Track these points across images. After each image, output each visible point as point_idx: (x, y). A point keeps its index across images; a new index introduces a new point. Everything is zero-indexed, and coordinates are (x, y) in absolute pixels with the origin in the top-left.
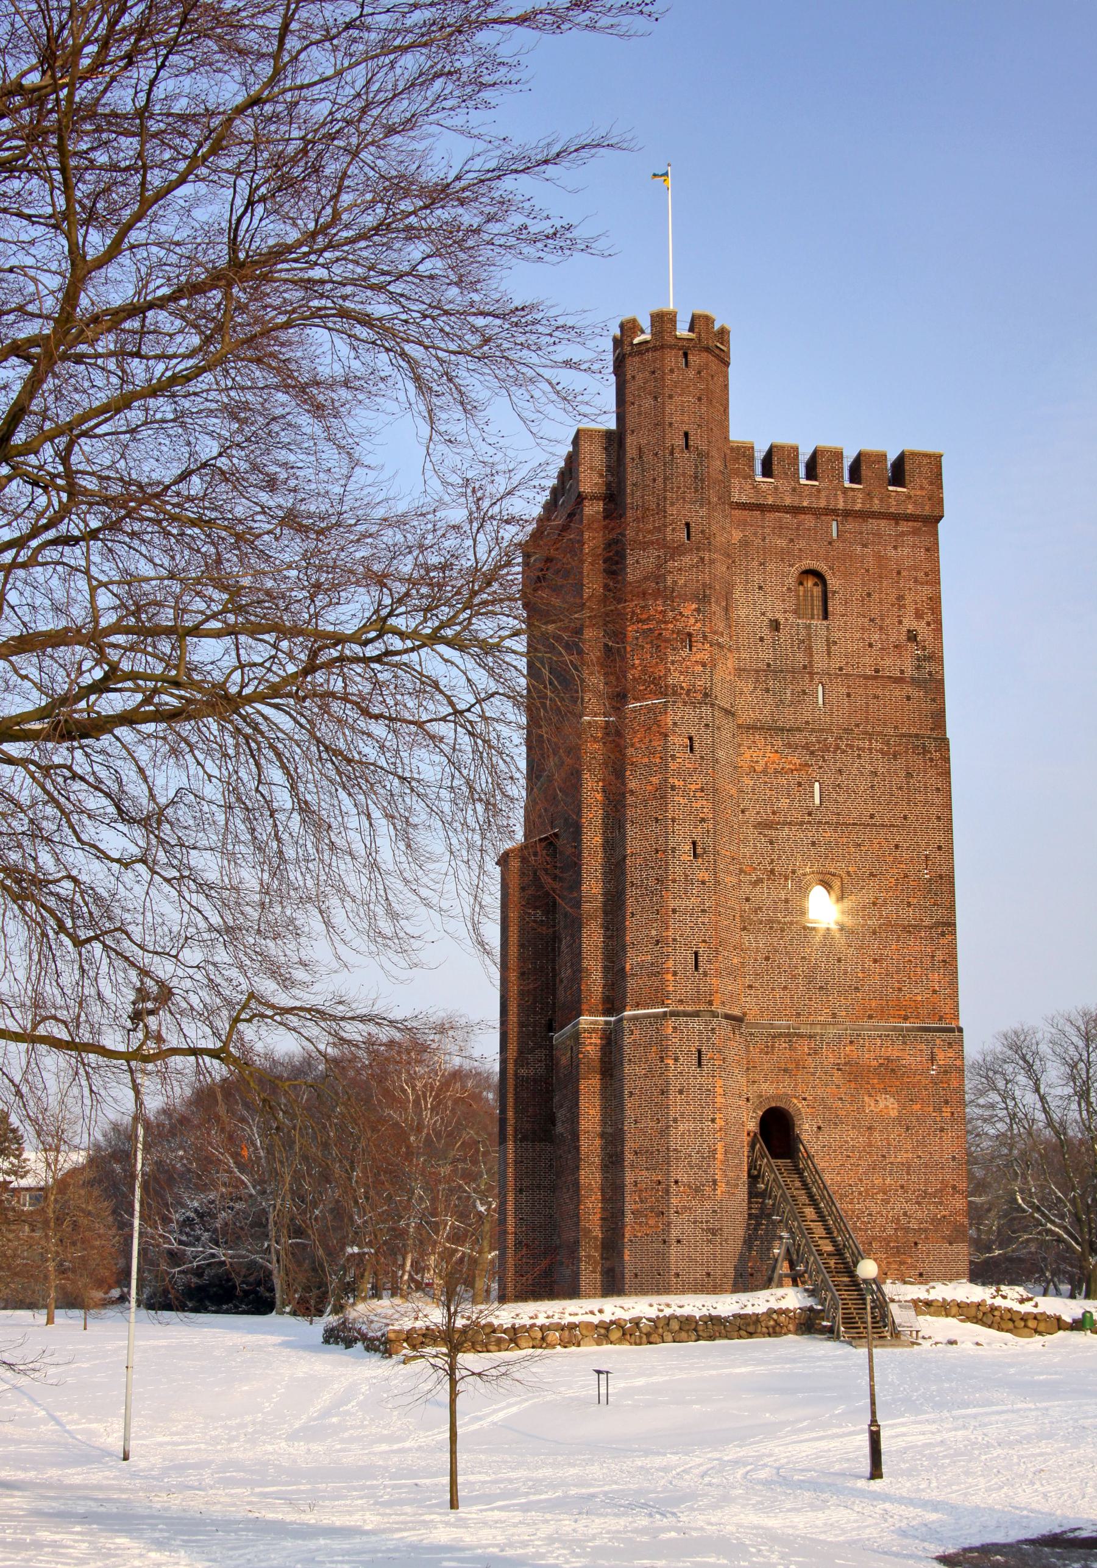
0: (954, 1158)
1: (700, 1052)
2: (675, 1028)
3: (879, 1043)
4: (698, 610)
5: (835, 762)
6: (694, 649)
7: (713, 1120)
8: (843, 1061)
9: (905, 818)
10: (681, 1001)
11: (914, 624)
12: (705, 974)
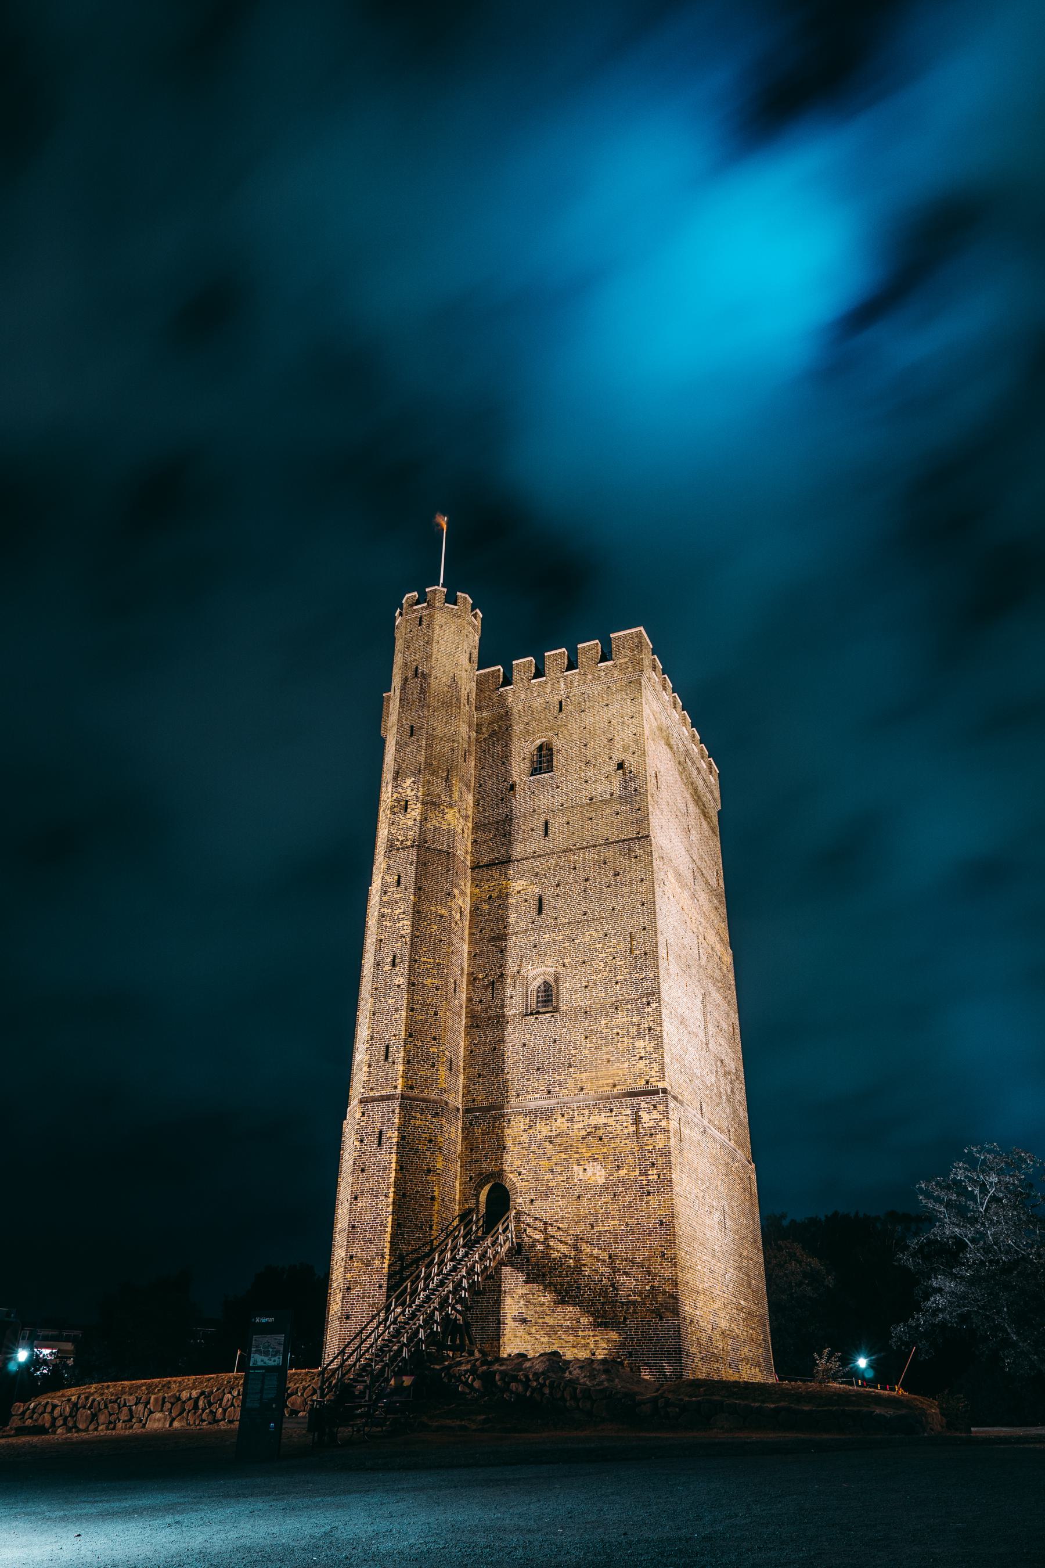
0: (661, 1221)
1: (381, 1132)
2: (363, 1114)
3: (586, 1112)
4: (414, 782)
5: (555, 876)
6: (409, 810)
7: (386, 1196)
8: (554, 1133)
9: (613, 909)
10: (372, 1089)
11: (623, 756)
12: (394, 1063)
